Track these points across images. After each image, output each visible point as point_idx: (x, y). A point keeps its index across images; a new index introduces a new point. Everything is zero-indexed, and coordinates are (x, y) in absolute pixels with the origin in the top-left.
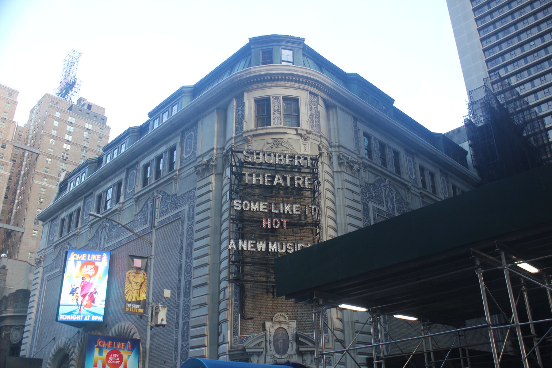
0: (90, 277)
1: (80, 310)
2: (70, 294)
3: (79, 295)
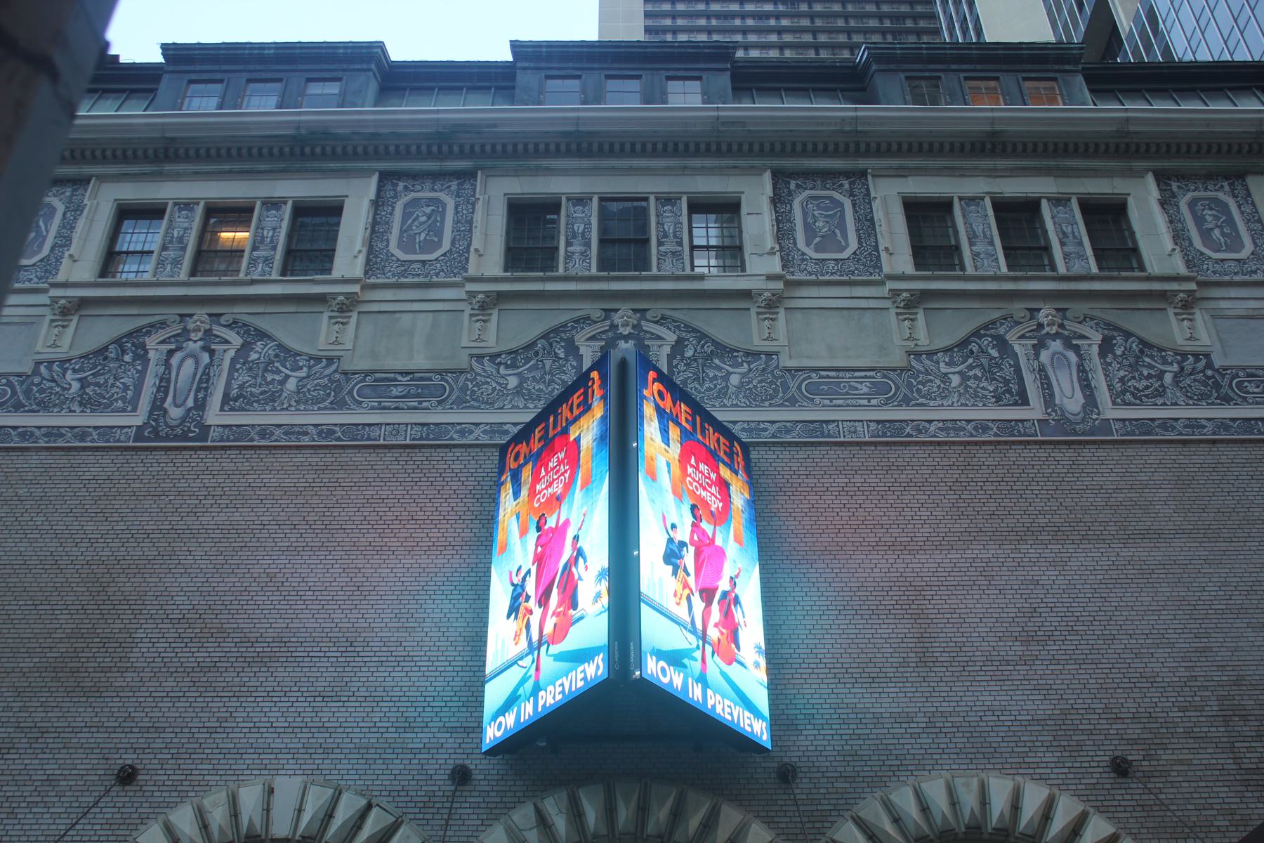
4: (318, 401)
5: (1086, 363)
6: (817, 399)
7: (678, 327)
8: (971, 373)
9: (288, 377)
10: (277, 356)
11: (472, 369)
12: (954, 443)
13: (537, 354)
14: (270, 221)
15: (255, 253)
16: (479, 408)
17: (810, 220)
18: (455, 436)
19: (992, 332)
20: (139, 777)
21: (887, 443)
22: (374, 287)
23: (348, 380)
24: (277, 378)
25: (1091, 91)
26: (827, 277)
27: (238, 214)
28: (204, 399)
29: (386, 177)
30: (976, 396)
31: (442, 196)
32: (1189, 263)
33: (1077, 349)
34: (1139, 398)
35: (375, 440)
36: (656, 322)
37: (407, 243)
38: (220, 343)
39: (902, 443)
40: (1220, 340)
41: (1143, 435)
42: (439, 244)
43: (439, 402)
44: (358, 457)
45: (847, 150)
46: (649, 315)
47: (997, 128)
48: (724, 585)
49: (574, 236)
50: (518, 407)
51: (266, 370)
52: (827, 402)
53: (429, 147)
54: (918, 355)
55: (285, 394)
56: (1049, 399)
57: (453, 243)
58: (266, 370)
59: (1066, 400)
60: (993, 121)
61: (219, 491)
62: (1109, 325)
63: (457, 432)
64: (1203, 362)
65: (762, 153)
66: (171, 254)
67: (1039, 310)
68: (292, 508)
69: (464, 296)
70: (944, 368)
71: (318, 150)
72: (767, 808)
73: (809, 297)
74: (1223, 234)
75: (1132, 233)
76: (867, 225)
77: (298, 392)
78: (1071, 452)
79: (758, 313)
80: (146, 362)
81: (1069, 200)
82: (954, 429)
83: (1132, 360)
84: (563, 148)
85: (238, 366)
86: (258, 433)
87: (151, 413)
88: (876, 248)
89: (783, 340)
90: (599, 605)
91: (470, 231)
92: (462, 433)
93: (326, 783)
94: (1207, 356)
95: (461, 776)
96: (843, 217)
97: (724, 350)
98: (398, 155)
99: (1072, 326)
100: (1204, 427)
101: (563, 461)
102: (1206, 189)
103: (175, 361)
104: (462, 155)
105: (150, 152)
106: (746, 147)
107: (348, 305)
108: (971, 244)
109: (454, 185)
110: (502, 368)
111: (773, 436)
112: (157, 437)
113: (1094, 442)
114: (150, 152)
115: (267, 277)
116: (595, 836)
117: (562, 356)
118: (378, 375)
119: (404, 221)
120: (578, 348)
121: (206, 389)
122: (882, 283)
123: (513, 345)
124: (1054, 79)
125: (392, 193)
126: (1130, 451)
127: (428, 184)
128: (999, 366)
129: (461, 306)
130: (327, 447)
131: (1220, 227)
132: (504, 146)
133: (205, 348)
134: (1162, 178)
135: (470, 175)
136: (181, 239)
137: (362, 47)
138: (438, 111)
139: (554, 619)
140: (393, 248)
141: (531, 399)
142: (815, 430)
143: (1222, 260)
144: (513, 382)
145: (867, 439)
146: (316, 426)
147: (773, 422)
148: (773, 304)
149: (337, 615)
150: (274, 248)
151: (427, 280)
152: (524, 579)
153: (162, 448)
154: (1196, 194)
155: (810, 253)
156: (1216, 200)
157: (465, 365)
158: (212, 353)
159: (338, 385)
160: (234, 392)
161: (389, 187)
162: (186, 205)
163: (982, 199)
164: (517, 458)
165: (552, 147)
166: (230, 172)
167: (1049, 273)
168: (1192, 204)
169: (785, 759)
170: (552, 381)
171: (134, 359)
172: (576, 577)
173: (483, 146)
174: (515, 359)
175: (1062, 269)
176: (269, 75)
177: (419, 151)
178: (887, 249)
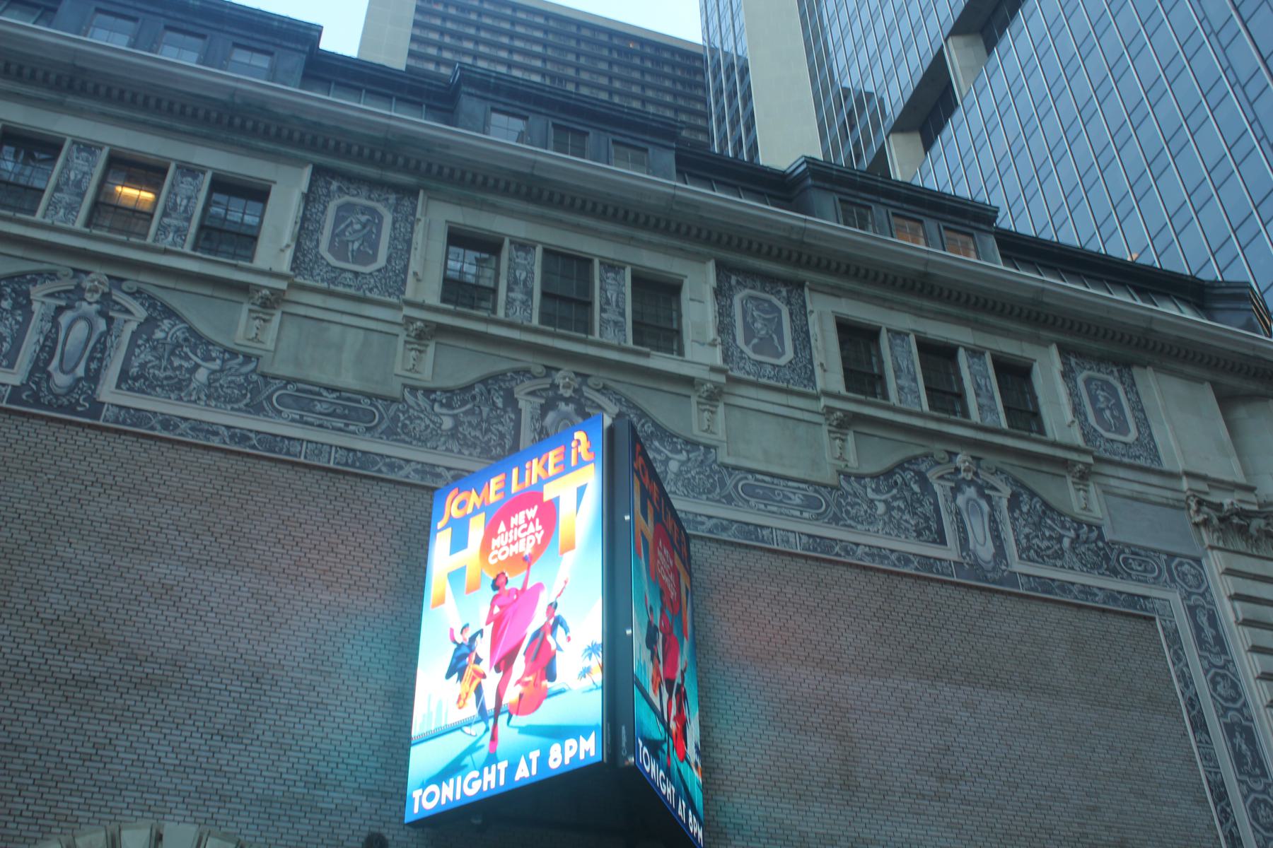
0: (526, 561)
1: (494, 739)
2: (449, 676)
3: (485, 666)
4: (230, 400)
5: (997, 515)
6: (753, 501)
7: (619, 401)
8: (895, 504)
9: (197, 366)
10: (186, 340)
11: (404, 399)
12: (878, 570)
13: (474, 398)
14: (186, 186)
15: (166, 220)
16: (411, 443)
17: (749, 319)
18: (384, 469)
19: (915, 467)
21: (817, 559)
22: (303, 288)
23: (267, 384)
24: (186, 364)
25: (1002, 256)
26: (764, 381)
27: (147, 172)
28: (98, 371)
29: (320, 172)
30: (899, 527)
31: (380, 207)
32: (1085, 436)
33: (989, 499)
34: (1040, 557)
35: (295, 456)
36: (598, 391)
37: (339, 247)
38: (119, 311)
39: (830, 561)
40: (1110, 515)
41: (1045, 594)
42: (374, 258)
43: (368, 429)
44: (275, 472)
45: (789, 257)
46: (591, 381)
47: (931, 270)
48: (678, 680)
49: (516, 281)
50: (452, 451)
51: (172, 353)
52: (762, 507)
53: (372, 152)
54: (847, 476)
55: (193, 385)
56: (964, 542)
57: (389, 260)
58: (172, 353)
59: (978, 547)
60: (927, 262)
61: (109, 480)
62: (1017, 482)
63: (385, 464)
64: (1095, 534)
65: (708, 241)
66: (65, 197)
67: (956, 454)
68: (195, 515)
69: (399, 319)
70: (871, 495)
71: (249, 124)
73: (748, 397)
74: (1113, 417)
75: (1034, 398)
76: (803, 338)
77: (209, 385)
78: (981, 599)
79: (699, 403)
80: (29, 314)
81: (983, 354)
82: (879, 556)
83: (1036, 519)
84: (513, 187)
85: (140, 342)
86: (161, 422)
87: (31, 374)
88: (811, 362)
89: (721, 435)
90: (587, 683)
91: (409, 251)
92: (391, 467)
94: (1099, 528)
96: (780, 324)
97: (663, 434)
98: (336, 152)
99: (985, 476)
100: (1096, 595)
101: (533, 521)
102: (1099, 371)
103: (64, 319)
104: (405, 169)
105: (52, 77)
106: (694, 231)
107: (271, 302)
108: (897, 377)
109: (392, 198)
110: (436, 406)
111: (710, 531)
112: (37, 403)
113: (1002, 592)
114: (52, 77)
115: (179, 249)
117: (500, 405)
118: (301, 386)
119: (336, 226)
120: (516, 402)
121: (101, 360)
122: (816, 398)
123: (450, 383)
124: (971, 235)
125: (325, 191)
126: (1034, 607)
127: (364, 191)
128: (920, 502)
129: (396, 330)
130: (239, 453)
131: (1111, 409)
132: (452, 170)
133: (101, 313)
134: (1064, 351)
135: (412, 192)
136: (78, 184)
137: (300, 26)
138: (390, 117)
139: (520, 689)
140: (323, 249)
141: (466, 444)
142: (750, 532)
143: (1112, 441)
144: (448, 423)
145: (799, 551)
146: (228, 427)
147: (710, 517)
148: (714, 396)
149: (243, 646)
150: (189, 220)
151: (360, 293)
152: (473, 639)
153: (42, 417)
154: (1091, 373)
155: (748, 351)
156: (1107, 383)
157: (397, 394)
158: (110, 321)
159: (256, 389)
160: (134, 371)
161: (321, 183)
162: (89, 147)
163: (908, 335)
164: (462, 505)
165: (502, 184)
166: (144, 123)
167: (959, 418)
168: (1088, 381)
170: (488, 430)
171: (14, 307)
172: (553, 647)
173: (430, 165)
174: (450, 400)
175: (975, 417)
176: (191, 28)
177: (360, 154)
178: (822, 365)
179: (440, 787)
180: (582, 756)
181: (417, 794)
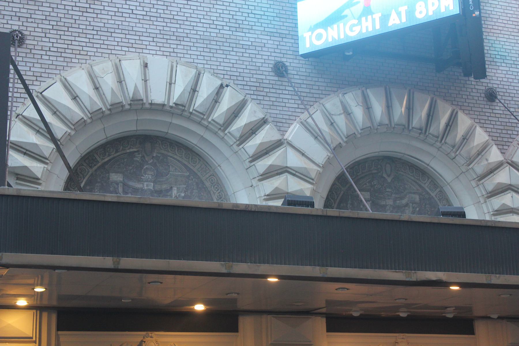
20: (27, 42)
72: (479, 117)
93: (188, 64)
95: (280, 70)
116: (380, 124)
169: (489, 85)
179: (326, 30)
180: (443, 10)
181: (307, 35)
